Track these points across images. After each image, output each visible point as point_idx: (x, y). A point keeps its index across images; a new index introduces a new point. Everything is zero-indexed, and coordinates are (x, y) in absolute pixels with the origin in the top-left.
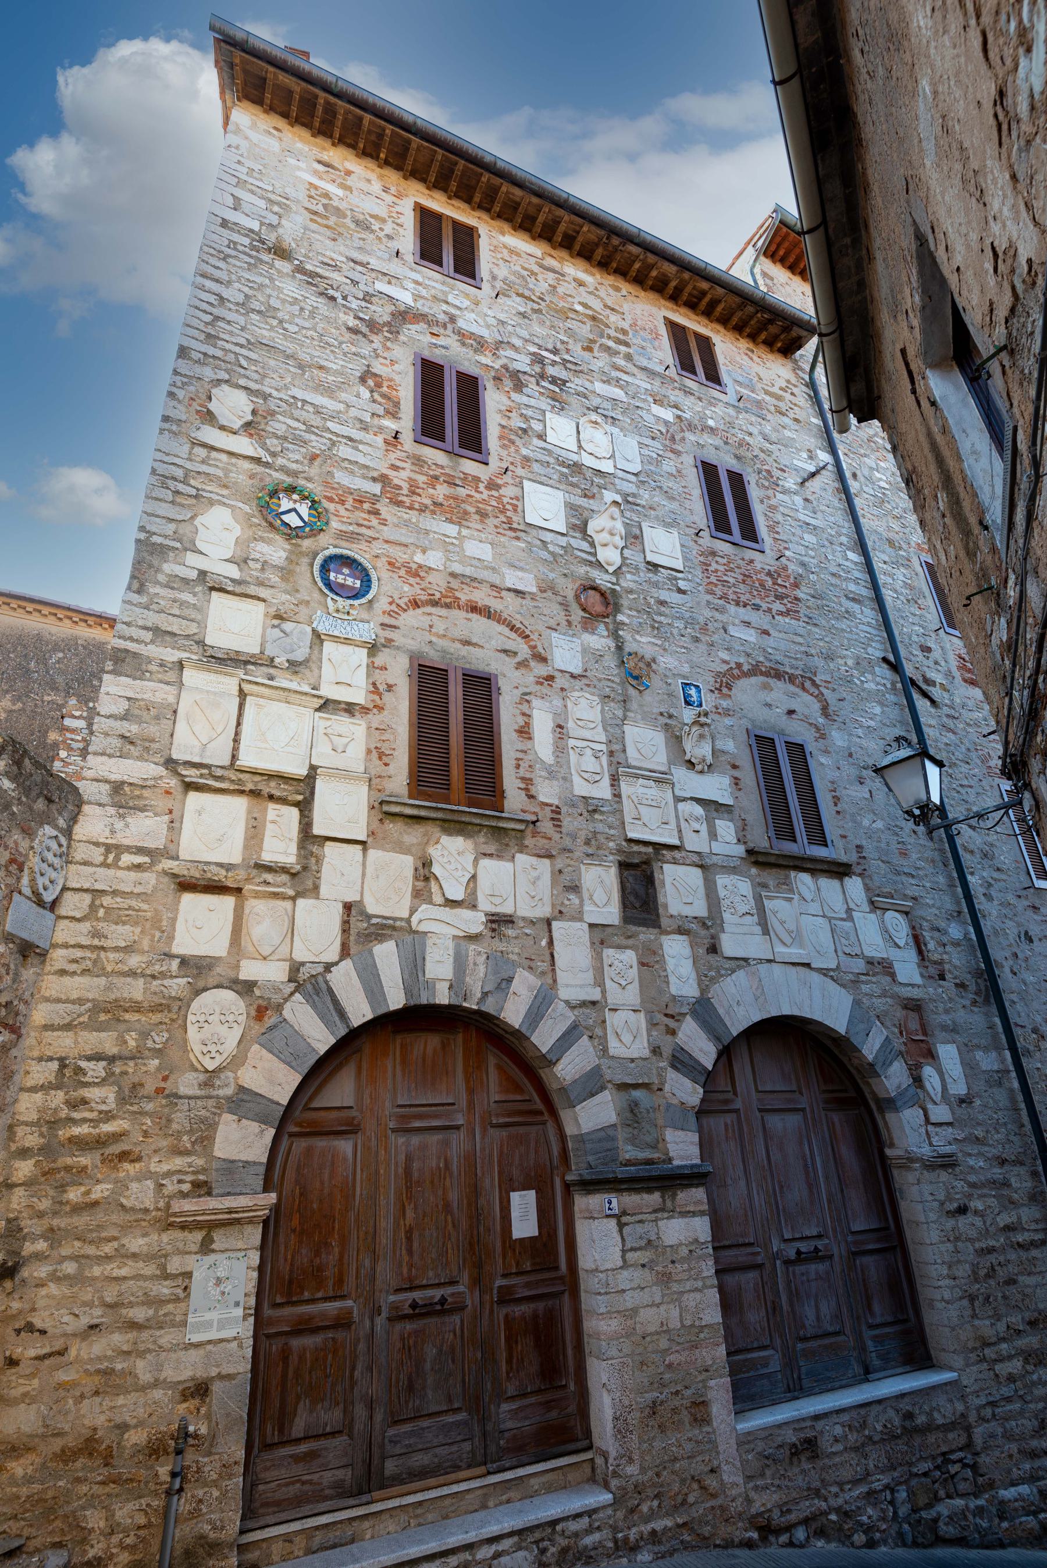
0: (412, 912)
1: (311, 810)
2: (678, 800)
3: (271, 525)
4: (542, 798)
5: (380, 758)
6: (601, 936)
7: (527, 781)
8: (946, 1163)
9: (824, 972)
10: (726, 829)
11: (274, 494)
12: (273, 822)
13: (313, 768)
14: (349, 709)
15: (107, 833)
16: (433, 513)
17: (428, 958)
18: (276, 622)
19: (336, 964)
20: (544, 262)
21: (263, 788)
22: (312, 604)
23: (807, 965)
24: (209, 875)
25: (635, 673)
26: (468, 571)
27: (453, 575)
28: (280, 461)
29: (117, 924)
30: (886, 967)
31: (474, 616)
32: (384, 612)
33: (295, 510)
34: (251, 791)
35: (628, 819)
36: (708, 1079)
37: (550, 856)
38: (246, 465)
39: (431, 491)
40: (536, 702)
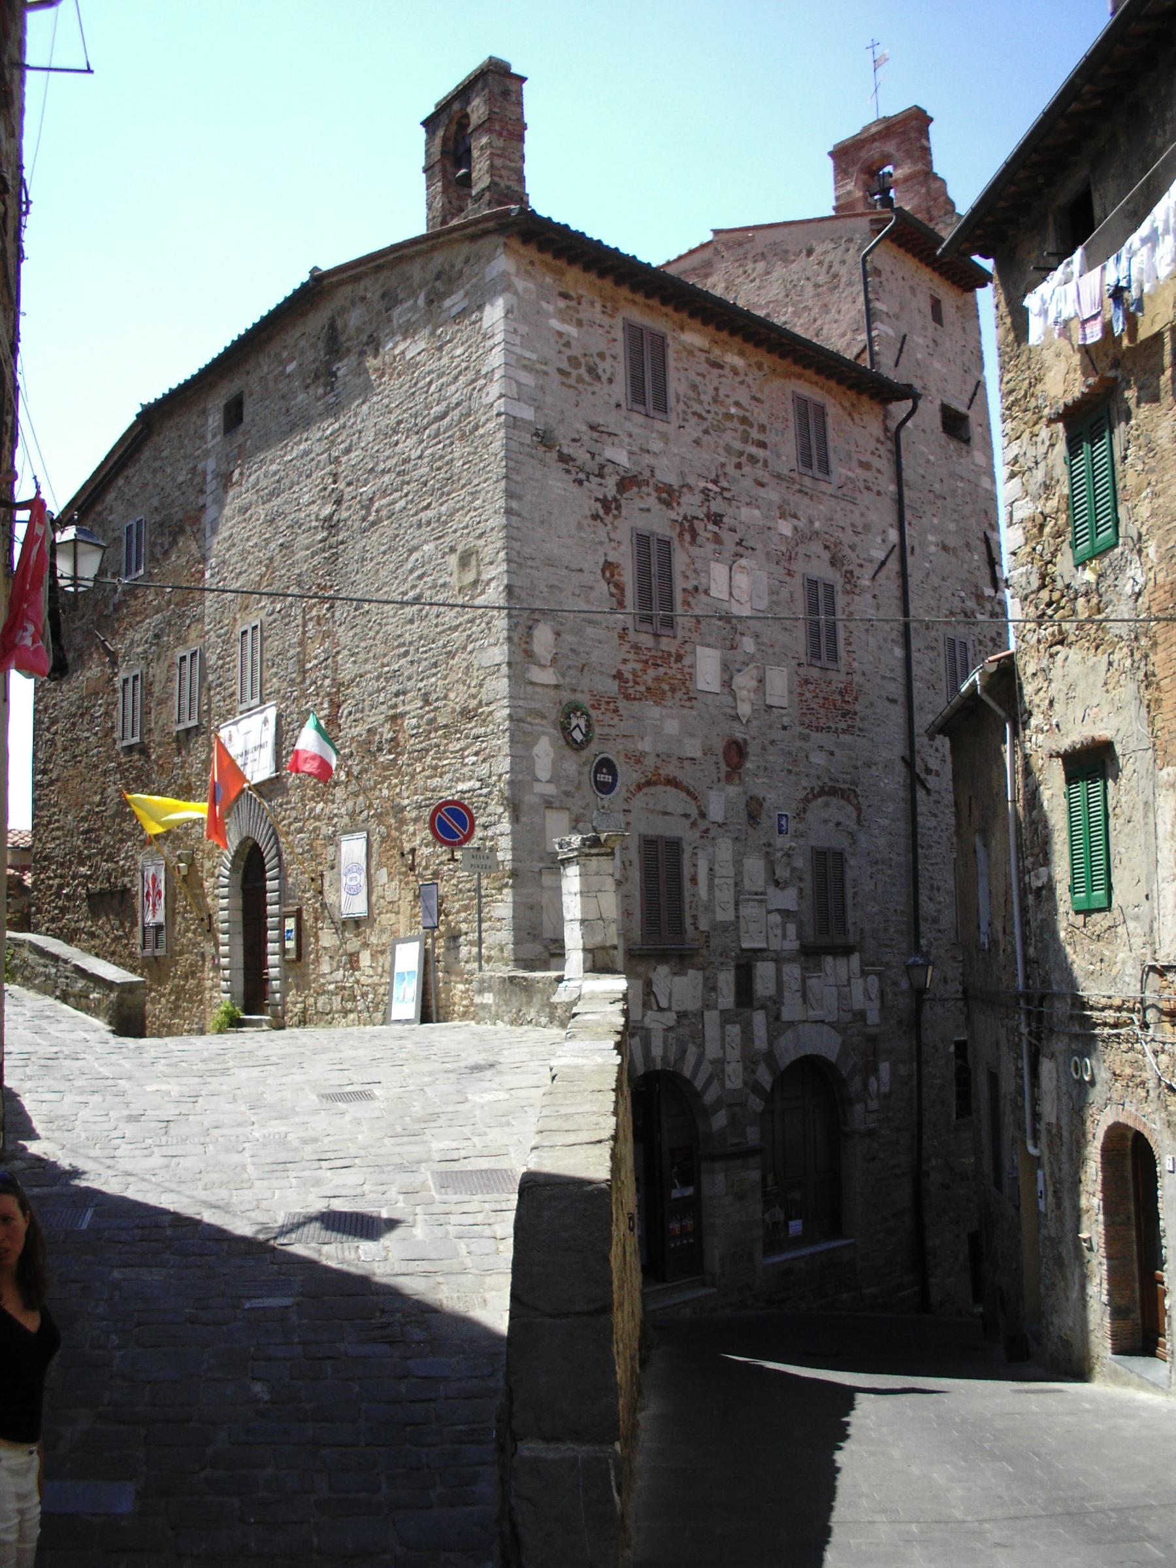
0: (643, 1016)
2: (769, 912)
3: (568, 743)
4: (702, 928)
6: (726, 1018)
7: (695, 917)
8: (871, 1133)
9: (830, 1024)
10: (792, 929)
20: (711, 356)
23: (822, 1022)
25: (754, 810)
30: (861, 1015)
31: (668, 788)
35: (742, 934)
36: (769, 1098)
37: (703, 969)
40: (700, 853)
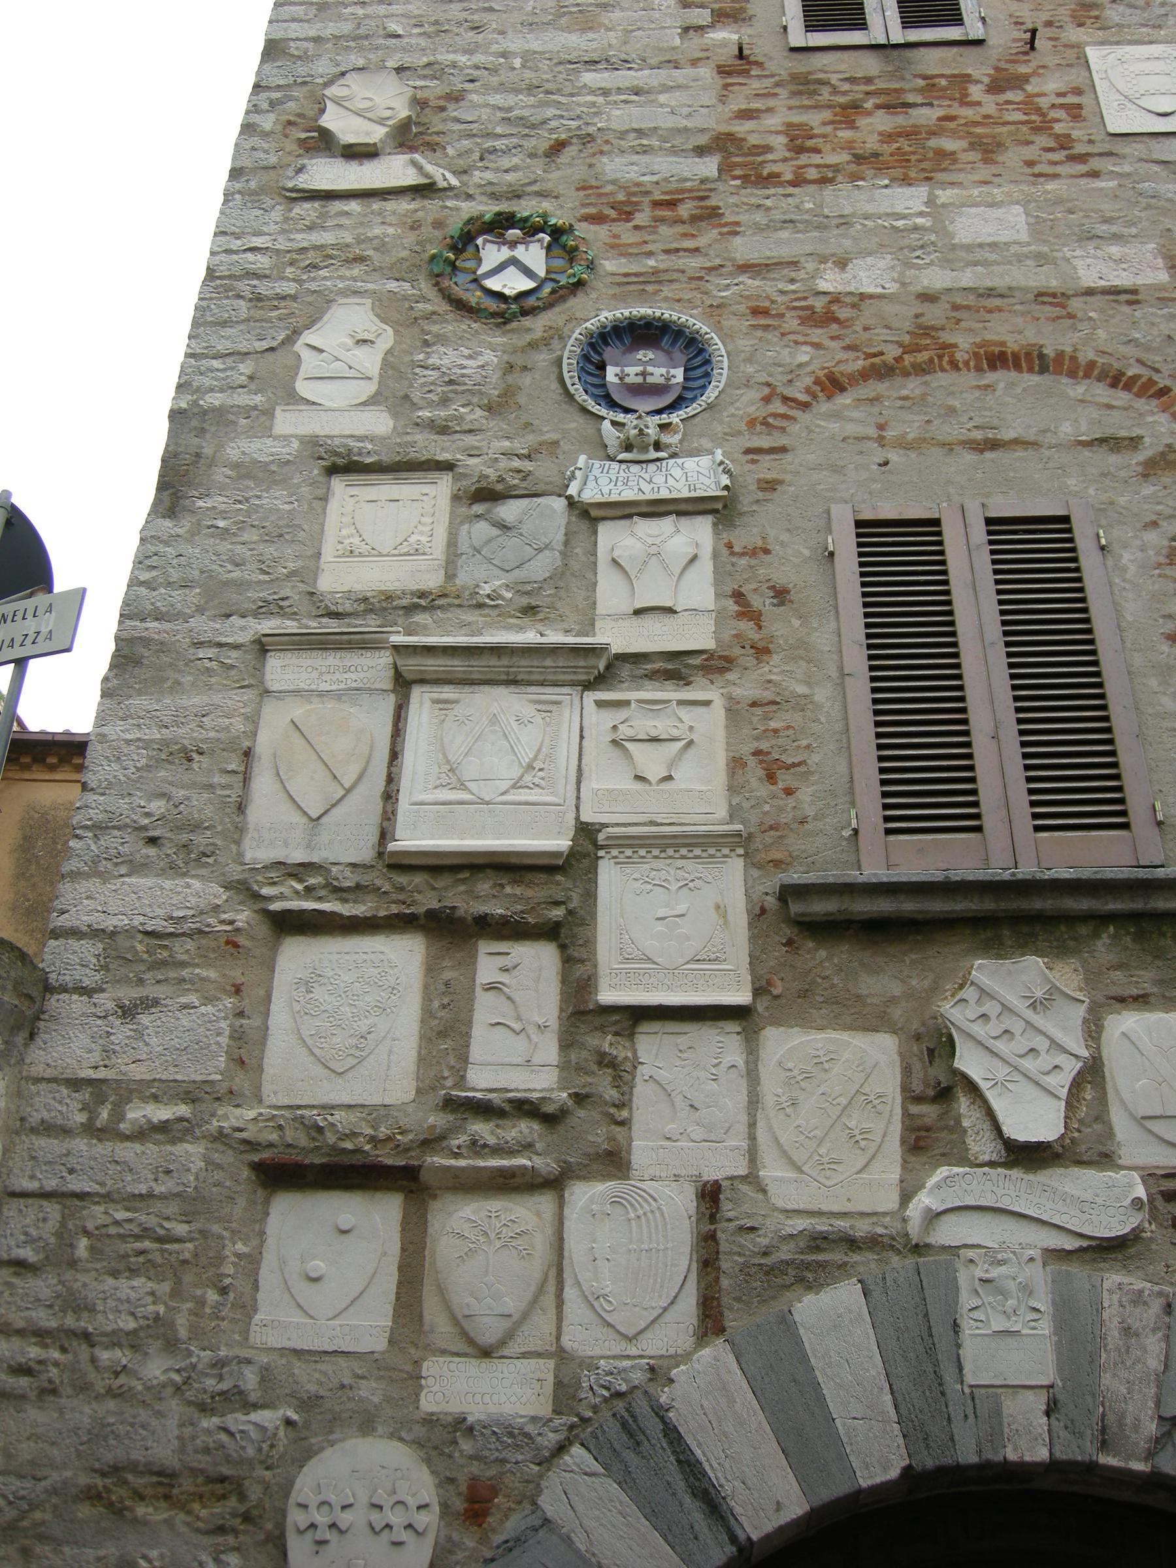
1: (590, 943)
5: (771, 778)
11: (464, 241)
12: (492, 987)
13: (586, 832)
14: (674, 667)
15: (96, 1058)
16: (855, 177)
17: (968, 1329)
18: (478, 508)
19: (686, 1357)
21: (464, 905)
22: (565, 446)
24: (331, 1138)
26: (968, 278)
27: (927, 297)
28: (478, 176)
29: (115, 1274)
32: (752, 423)
33: (514, 262)
34: (431, 914)
38: (404, 205)
39: (845, 134)
